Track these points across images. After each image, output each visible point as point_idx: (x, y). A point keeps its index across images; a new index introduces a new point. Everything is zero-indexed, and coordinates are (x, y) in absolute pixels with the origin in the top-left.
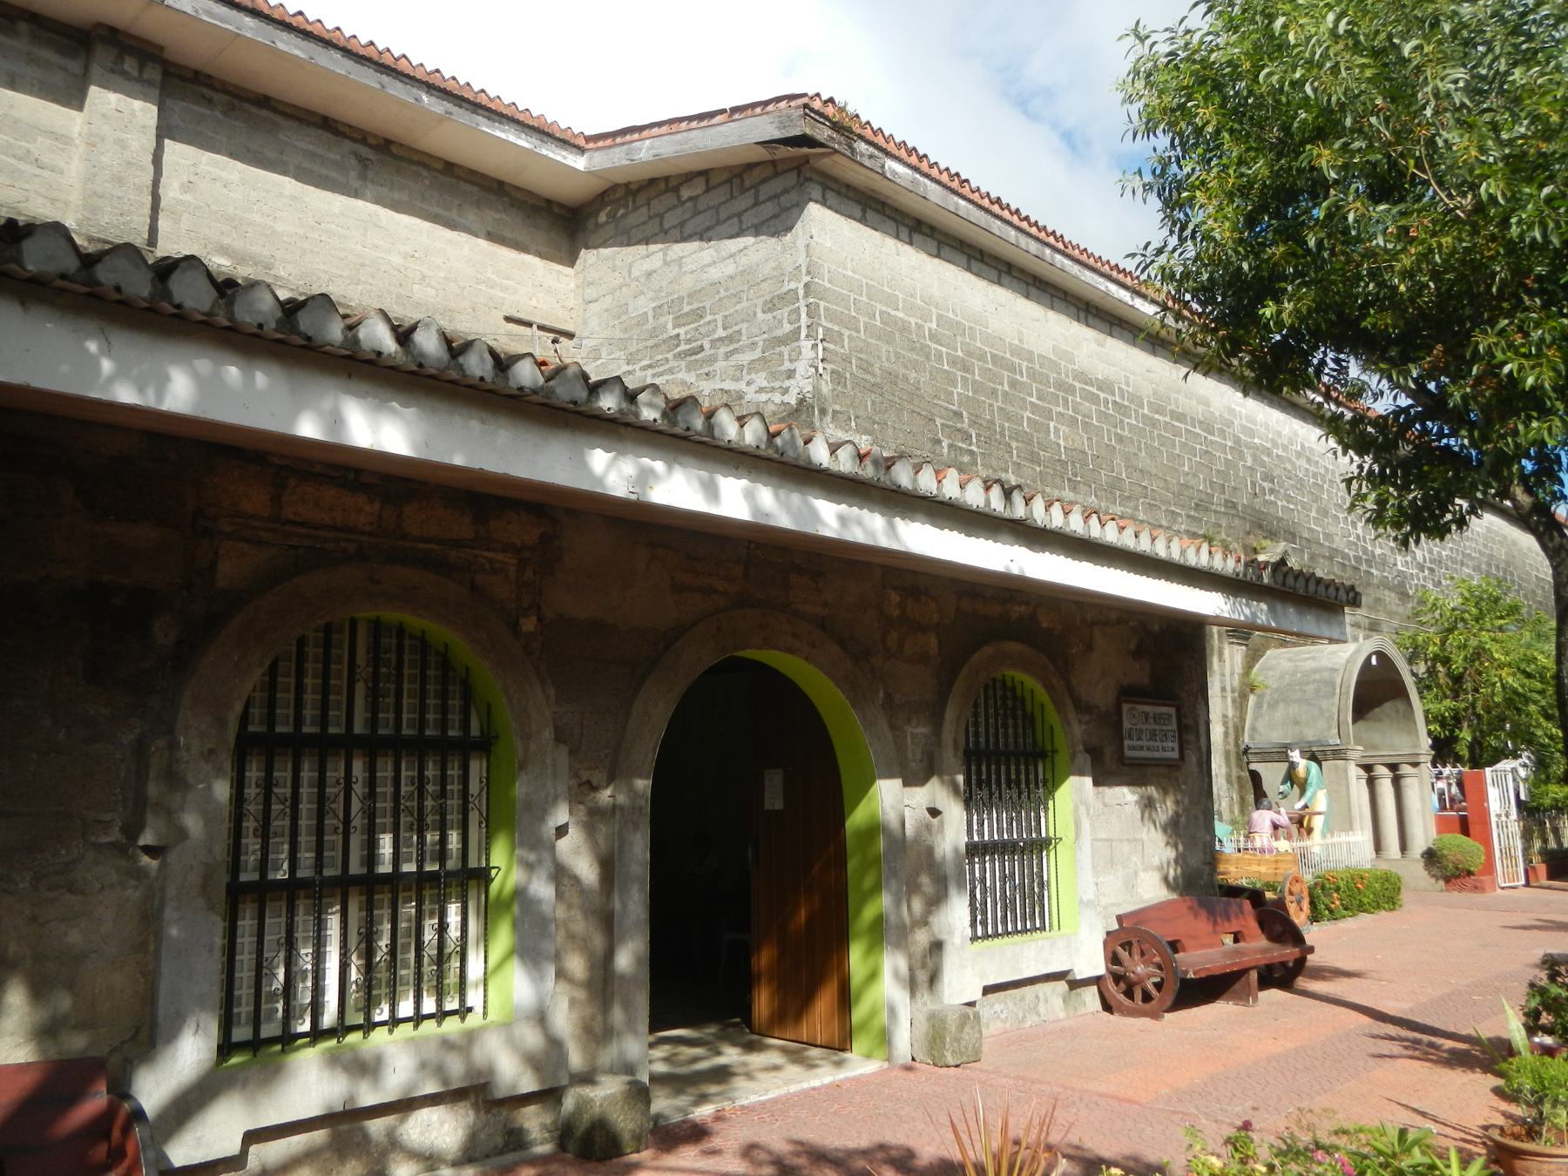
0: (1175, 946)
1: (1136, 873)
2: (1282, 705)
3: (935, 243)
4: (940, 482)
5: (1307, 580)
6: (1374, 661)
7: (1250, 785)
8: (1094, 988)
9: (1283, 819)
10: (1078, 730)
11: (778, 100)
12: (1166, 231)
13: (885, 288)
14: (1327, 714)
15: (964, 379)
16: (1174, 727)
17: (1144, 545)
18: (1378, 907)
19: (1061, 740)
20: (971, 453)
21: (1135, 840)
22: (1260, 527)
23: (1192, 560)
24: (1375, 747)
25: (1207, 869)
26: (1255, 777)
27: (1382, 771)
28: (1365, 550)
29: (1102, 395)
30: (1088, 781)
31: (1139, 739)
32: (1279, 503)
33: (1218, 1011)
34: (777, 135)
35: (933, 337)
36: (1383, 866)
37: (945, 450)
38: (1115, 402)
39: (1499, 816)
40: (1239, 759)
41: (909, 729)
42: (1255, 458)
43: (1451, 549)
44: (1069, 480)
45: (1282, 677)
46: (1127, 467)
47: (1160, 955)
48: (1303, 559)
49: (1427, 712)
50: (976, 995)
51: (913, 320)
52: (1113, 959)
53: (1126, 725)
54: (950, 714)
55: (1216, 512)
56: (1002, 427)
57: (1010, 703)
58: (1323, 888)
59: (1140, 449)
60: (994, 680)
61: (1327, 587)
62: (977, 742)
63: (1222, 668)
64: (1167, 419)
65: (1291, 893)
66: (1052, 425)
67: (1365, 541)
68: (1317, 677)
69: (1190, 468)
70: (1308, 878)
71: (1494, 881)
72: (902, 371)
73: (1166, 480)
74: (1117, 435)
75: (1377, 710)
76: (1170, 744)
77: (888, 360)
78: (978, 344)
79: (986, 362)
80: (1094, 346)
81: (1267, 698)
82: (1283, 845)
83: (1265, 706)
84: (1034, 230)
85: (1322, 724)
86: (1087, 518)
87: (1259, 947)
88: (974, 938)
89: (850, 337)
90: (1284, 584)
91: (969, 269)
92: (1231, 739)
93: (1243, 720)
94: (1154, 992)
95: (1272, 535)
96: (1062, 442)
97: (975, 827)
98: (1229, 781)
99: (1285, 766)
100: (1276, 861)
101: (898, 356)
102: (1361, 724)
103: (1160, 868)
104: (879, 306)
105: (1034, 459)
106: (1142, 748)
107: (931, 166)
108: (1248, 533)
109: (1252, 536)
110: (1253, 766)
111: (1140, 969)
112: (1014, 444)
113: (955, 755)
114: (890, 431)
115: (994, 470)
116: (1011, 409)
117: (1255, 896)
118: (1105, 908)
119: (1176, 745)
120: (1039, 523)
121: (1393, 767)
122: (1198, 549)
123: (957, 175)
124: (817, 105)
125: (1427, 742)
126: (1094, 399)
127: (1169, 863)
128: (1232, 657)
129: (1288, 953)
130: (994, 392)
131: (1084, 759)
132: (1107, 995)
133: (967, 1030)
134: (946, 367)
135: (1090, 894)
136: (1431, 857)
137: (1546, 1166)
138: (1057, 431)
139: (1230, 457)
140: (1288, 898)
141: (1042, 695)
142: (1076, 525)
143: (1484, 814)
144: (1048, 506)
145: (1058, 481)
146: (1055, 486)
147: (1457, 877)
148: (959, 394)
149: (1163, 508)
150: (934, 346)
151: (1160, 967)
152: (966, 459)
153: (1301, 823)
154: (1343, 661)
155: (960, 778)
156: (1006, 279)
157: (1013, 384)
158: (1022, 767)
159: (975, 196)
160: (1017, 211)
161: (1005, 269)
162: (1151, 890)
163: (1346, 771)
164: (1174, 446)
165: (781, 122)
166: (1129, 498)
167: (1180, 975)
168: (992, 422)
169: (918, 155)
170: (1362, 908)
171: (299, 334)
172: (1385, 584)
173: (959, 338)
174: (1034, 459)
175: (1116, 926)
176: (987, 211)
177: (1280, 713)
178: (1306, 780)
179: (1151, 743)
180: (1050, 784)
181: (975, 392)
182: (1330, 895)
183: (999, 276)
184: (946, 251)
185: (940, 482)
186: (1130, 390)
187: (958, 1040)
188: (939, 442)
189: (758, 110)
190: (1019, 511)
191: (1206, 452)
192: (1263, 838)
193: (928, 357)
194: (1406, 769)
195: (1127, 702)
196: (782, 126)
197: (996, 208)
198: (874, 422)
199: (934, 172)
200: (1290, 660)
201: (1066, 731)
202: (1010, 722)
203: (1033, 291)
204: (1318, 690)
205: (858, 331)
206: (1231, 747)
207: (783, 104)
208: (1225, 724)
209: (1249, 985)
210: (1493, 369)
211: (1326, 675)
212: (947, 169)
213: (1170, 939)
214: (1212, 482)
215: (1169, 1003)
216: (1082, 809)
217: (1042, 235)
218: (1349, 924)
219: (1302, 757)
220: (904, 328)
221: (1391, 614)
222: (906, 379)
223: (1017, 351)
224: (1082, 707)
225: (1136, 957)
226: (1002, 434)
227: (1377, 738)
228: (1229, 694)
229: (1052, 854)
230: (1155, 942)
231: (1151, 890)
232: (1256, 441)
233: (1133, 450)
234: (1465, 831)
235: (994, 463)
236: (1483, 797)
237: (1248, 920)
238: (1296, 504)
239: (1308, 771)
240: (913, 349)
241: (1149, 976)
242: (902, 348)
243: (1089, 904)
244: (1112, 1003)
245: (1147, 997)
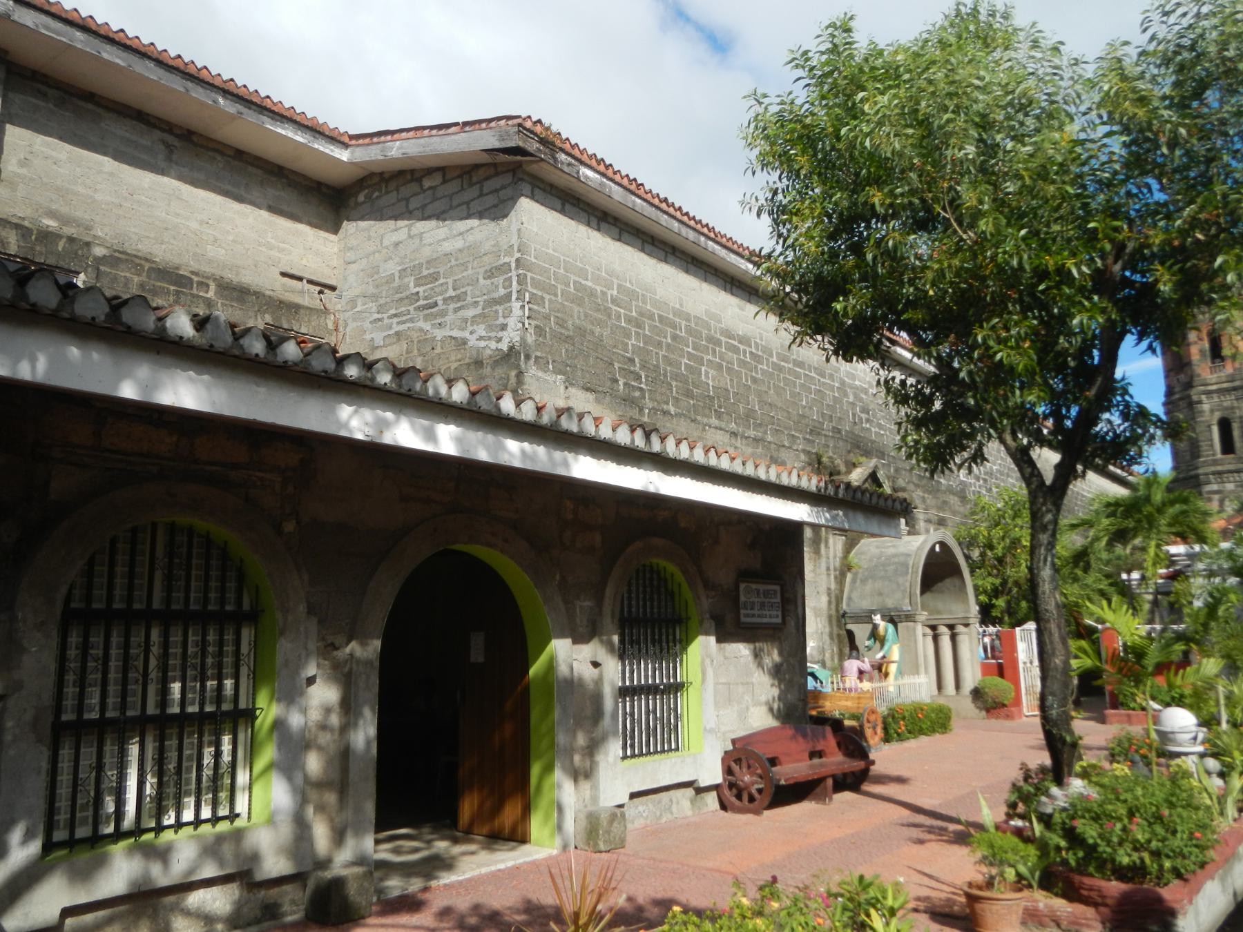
0: (773, 762)
1: (747, 709)
2: (870, 581)
3: (618, 230)
4: (597, 426)
5: (871, 495)
7: (846, 640)
8: (714, 794)
9: (866, 666)
10: (706, 603)
11: (499, 119)
12: (774, 241)
13: (578, 264)
15: (637, 334)
16: (778, 600)
17: (749, 471)
18: (934, 731)
19: (693, 611)
20: (641, 389)
21: (748, 683)
22: (858, 447)
23: (785, 481)
24: (938, 612)
25: (801, 704)
26: (850, 635)
27: (943, 630)
29: (742, 347)
30: (712, 639)
31: (752, 609)
32: (873, 430)
33: (806, 807)
34: (497, 145)
35: (614, 301)
36: (942, 701)
37: (621, 387)
38: (751, 353)
39: (1025, 663)
40: (839, 621)
41: (578, 603)
42: (856, 396)
43: (1000, 465)
44: (715, 411)
45: (871, 560)
46: (759, 402)
47: (762, 768)
48: (889, 471)
49: (976, 588)
50: (624, 799)
51: (599, 288)
52: (728, 771)
53: (742, 599)
54: (609, 592)
55: (825, 436)
56: (665, 370)
57: (655, 583)
58: (893, 717)
59: (769, 388)
60: (644, 566)
61: (886, 500)
62: (630, 612)
63: (827, 554)
64: (791, 366)
65: (868, 721)
66: (703, 369)
68: (896, 560)
69: (807, 403)
70: (883, 709)
71: (1020, 711)
72: (589, 327)
73: (788, 412)
74: (752, 377)
76: (775, 613)
77: (579, 318)
78: (649, 307)
79: (653, 320)
80: (737, 310)
81: (860, 576)
82: (866, 685)
84: (692, 223)
85: (898, 595)
86: (707, 452)
87: (836, 761)
88: (625, 757)
89: (550, 300)
90: (854, 498)
91: (643, 250)
92: (833, 606)
93: (842, 591)
94: (756, 795)
95: (867, 454)
96: (711, 384)
97: (627, 675)
98: (831, 637)
99: (870, 627)
100: (859, 698)
101: (586, 316)
102: (928, 595)
103: (767, 703)
104: (573, 277)
105: (689, 394)
106: (753, 616)
107: (615, 173)
108: (849, 452)
109: (852, 454)
110: (849, 627)
111: (747, 778)
112: (674, 383)
113: (613, 622)
114: (579, 373)
115: (659, 403)
116: (672, 356)
117: (837, 725)
118: (724, 734)
119: (780, 613)
120: (671, 455)
121: (951, 627)
122: (790, 473)
123: (635, 180)
124: (528, 124)
125: (975, 609)
126: (735, 350)
127: (774, 698)
128: (835, 544)
129: (858, 765)
130: (660, 344)
131: (709, 624)
132: (723, 798)
133: (615, 824)
134: (623, 324)
135: (711, 724)
136: (977, 693)
137: (994, 908)
138: (707, 373)
139: (836, 395)
140: (866, 725)
141: (679, 577)
142: (699, 456)
143: (1014, 662)
144: (678, 442)
145: (707, 411)
146: (704, 415)
147: (995, 708)
148: (633, 345)
149: (786, 432)
150: (614, 308)
151: (761, 777)
152: (637, 394)
153: (880, 669)
154: (914, 548)
155: (616, 638)
156: (670, 258)
157: (675, 337)
158: (664, 630)
159: (649, 197)
160: (680, 209)
161: (670, 251)
162: (760, 719)
163: (914, 630)
164: (795, 386)
165: (501, 136)
166: (760, 425)
167: (775, 782)
168: (657, 366)
169: (605, 164)
170: (921, 732)
171: (122, 324)
172: (950, 490)
173: (634, 303)
174: (689, 394)
175: (731, 747)
176: (657, 208)
177: (869, 587)
178: (884, 637)
179: (760, 612)
180: (684, 643)
181: (645, 343)
182: (898, 723)
183: (666, 256)
184: (625, 236)
185: (597, 426)
186: (763, 343)
187: (608, 832)
188: (616, 381)
189: (484, 125)
190: (656, 447)
191: (819, 391)
192: (852, 681)
193: (609, 316)
194: (960, 629)
195: (743, 582)
196: (501, 138)
197: (664, 206)
198: (567, 365)
199: (617, 178)
200: (877, 547)
201: (696, 602)
202: (655, 597)
203: (691, 267)
204: (896, 570)
205: (556, 295)
206: (833, 612)
207: (503, 122)
208: (829, 595)
209: (826, 788)
210: (988, 355)
211: (902, 559)
212: (627, 176)
213: (770, 756)
214: (823, 413)
215: (766, 803)
216: (708, 661)
217: (699, 227)
218: (912, 744)
219: (883, 618)
220: (592, 294)
221: (954, 513)
222: (592, 333)
223: (678, 313)
224: (709, 585)
225: (745, 770)
226: (665, 375)
227: (940, 605)
228: (832, 572)
229: (685, 694)
230: (758, 758)
231: (760, 719)
232: (857, 383)
233: (764, 388)
234: (1001, 675)
235: (658, 398)
236: (1014, 649)
237: (829, 742)
238: (885, 431)
239: (886, 630)
240: (599, 310)
241: (753, 784)
242: (590, 309)
243: (711, 731)
244: (727, 804)
245: (752, 799)
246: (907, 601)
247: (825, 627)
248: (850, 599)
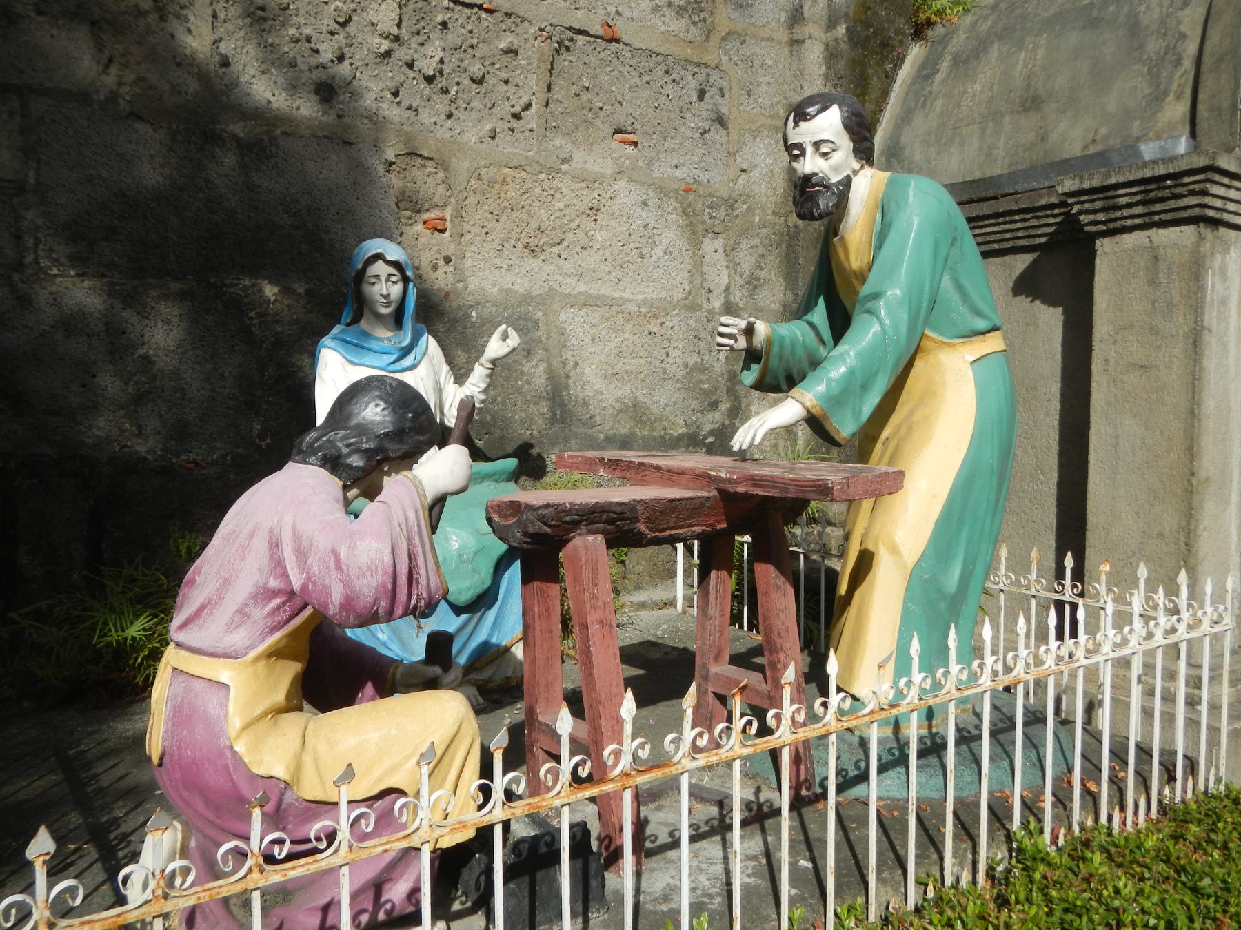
2: (995, 51)
14: (1153, 46)
81: (959, 41)
83: (945, 65)
246: (1177, 110)
247: (753, 284)
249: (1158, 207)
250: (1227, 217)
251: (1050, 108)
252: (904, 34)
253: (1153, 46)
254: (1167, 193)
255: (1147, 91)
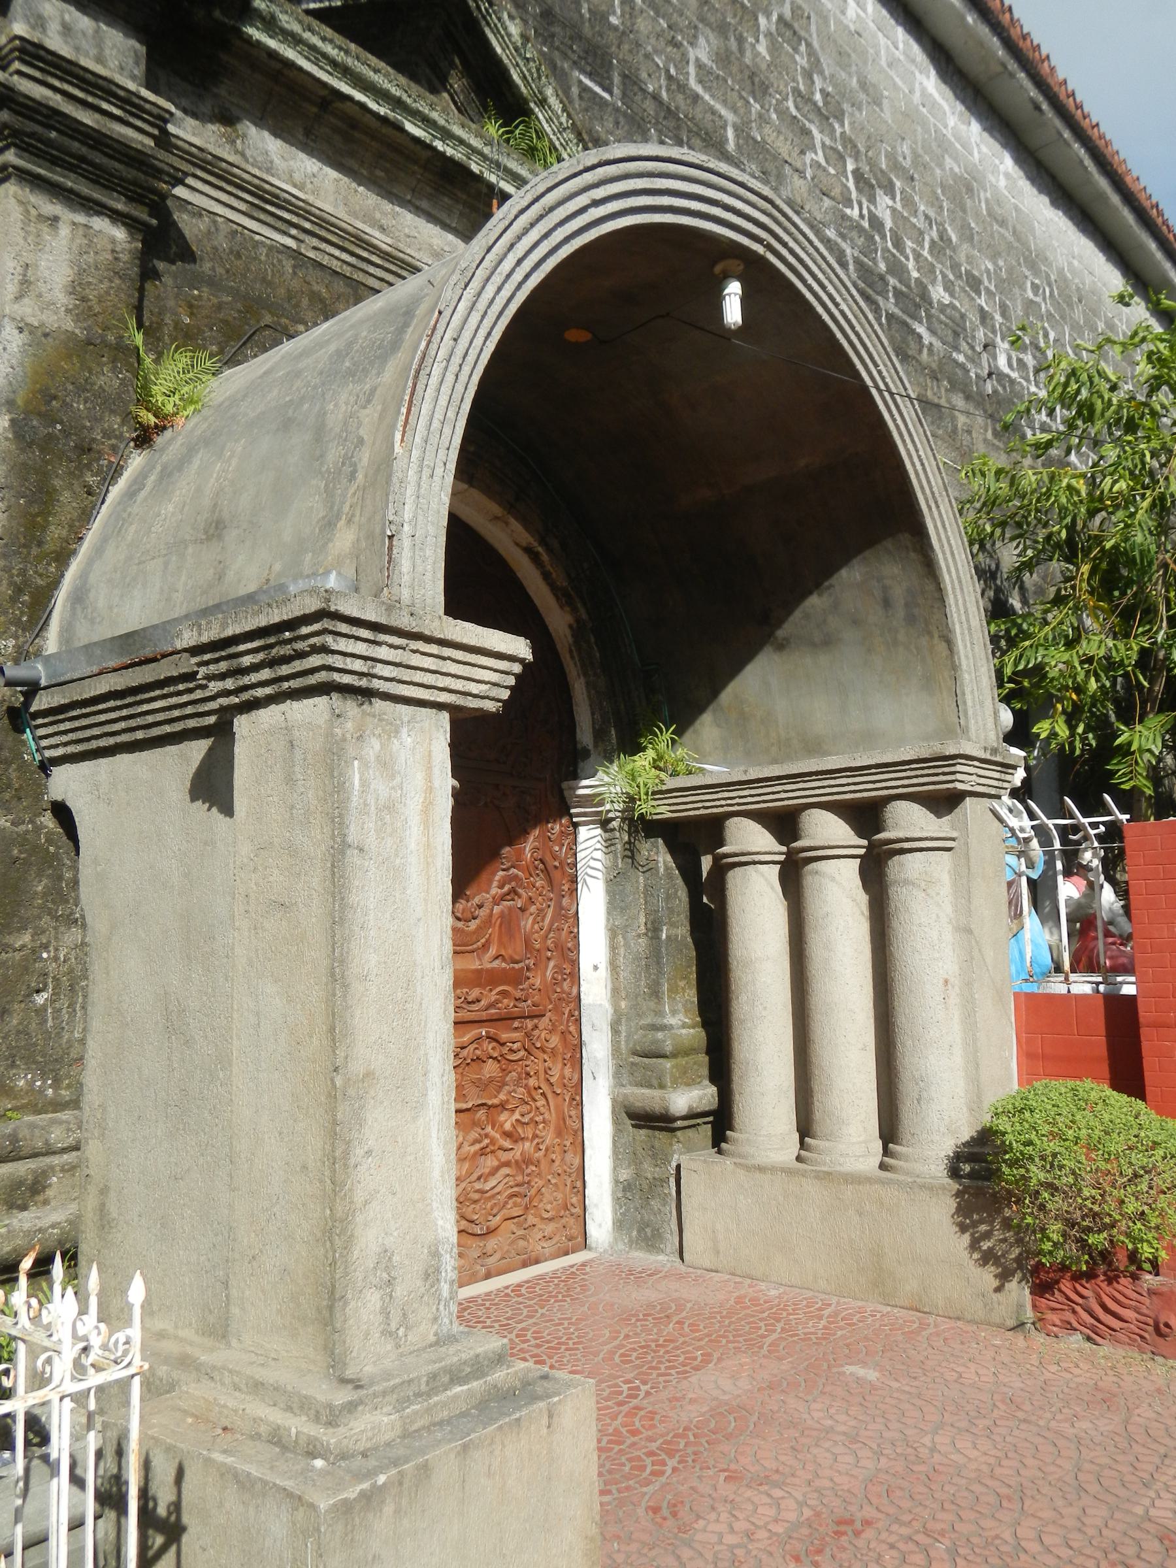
2: (196, 462)
6: (733, 312)
14: (334, 454)
24: (814, 747)
28: (897, 269)
67: (898, 244)
75: (814, 601)
248: (79, 597)
249: (285, 670)
250: (377, 684)
251: (231, 535)
252: (120, 437)
253: (334, 454)
254: (286, 650)
255: (321, 515)
